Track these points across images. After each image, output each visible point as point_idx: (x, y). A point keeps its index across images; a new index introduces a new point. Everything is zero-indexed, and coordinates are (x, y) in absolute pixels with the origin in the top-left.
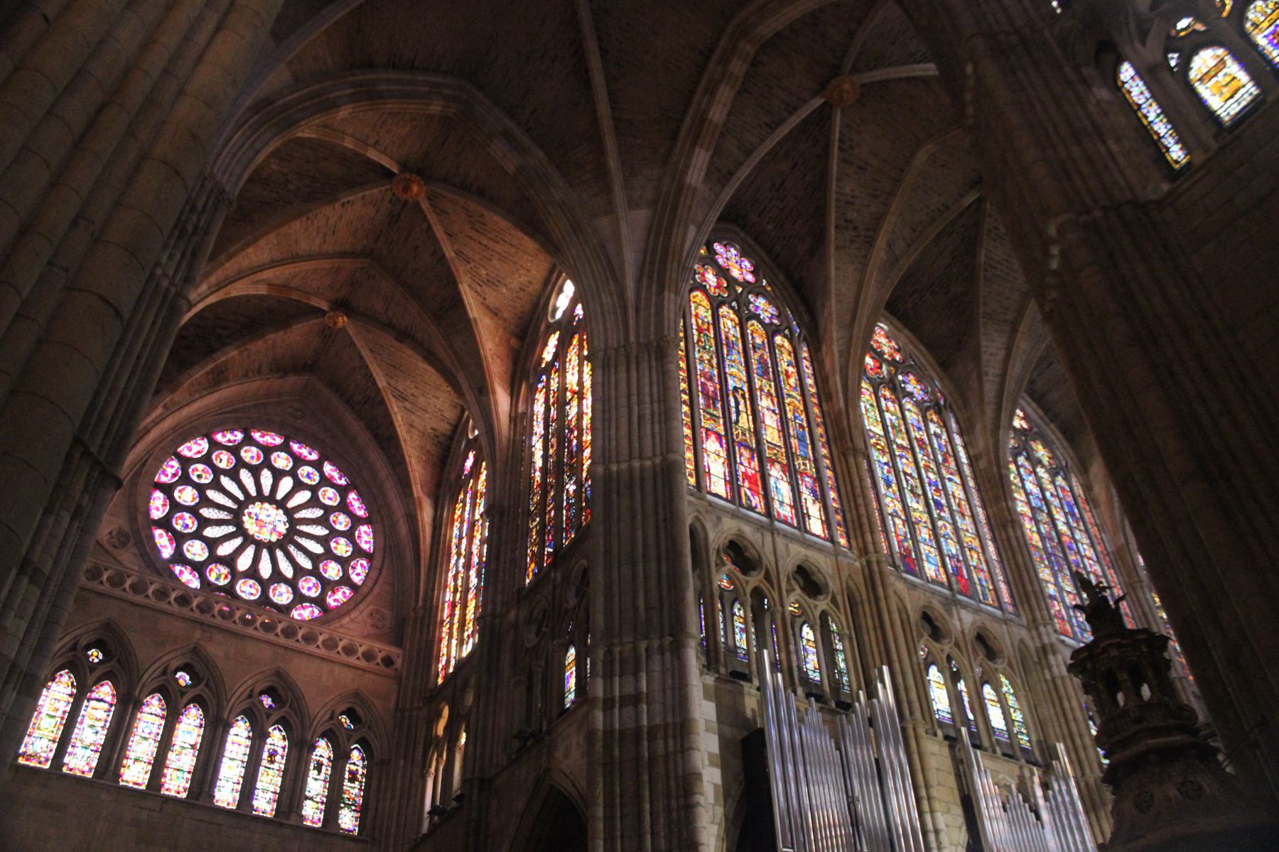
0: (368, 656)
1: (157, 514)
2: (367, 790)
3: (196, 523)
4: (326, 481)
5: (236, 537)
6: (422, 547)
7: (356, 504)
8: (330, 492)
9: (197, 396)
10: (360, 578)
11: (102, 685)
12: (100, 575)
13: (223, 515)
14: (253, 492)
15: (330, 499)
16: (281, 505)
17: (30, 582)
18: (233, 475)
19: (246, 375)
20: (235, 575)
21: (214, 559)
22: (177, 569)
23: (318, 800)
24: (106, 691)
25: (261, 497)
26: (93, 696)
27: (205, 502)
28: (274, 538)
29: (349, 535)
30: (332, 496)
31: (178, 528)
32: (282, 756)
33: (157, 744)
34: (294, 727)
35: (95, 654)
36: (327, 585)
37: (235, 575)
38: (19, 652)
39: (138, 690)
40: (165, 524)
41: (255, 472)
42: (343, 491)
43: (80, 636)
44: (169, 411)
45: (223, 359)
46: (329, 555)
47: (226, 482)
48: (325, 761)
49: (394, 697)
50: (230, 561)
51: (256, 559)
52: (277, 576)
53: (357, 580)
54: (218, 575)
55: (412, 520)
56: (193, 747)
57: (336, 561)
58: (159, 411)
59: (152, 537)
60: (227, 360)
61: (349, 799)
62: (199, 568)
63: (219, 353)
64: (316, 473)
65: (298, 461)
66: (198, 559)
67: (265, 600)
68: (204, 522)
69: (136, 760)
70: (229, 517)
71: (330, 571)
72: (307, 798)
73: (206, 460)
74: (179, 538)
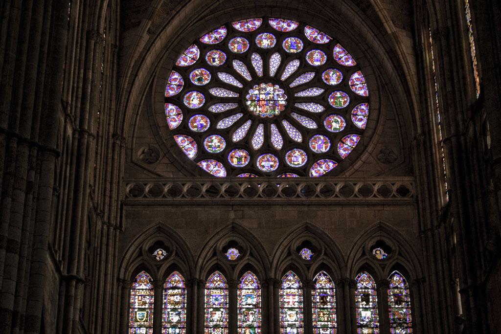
0: (384, 191)
1: (174, 125)
4: (310, 45)
5: (245, 122)
6: (408, 78)
9: (174, 12)
10: (363, 122)
12: (143, 190)
16: (275, 80)
17: (7, 252)
18: (228, 68)
20: (253, 155)
21: (232, 146)
22: (204, 164)
24: (177, 278)
25: (257, 80)
26: (169, 285)
27: (211, 100)
34: (333, 270)
35: (160, 252)
36: (335, 138)
38: (15, 302)
39: (198, 273)
40: (183, 130)
41: (245, 59)
42: (327, 49)
43: (142, 243)
44: (154, 34)
46: (330, 111)
49: (415, 222)
50: (245, 144)
51: (267, 135)
52: (289, 144)
53: (360, 124)
54: (238, 158)
55: (392, 54)
56: (256, 306)
57: (337, 114)
58: (146, 37)
59: (175, 144)
61: (399, 319)
62: (221, 158)
64: (299, 41)
65: (281, 36)
66: (218, 150)
67: (284, 168)
68: (215, 118)
71: (334, 124)
72: (362, 326)
74: (198, 138)
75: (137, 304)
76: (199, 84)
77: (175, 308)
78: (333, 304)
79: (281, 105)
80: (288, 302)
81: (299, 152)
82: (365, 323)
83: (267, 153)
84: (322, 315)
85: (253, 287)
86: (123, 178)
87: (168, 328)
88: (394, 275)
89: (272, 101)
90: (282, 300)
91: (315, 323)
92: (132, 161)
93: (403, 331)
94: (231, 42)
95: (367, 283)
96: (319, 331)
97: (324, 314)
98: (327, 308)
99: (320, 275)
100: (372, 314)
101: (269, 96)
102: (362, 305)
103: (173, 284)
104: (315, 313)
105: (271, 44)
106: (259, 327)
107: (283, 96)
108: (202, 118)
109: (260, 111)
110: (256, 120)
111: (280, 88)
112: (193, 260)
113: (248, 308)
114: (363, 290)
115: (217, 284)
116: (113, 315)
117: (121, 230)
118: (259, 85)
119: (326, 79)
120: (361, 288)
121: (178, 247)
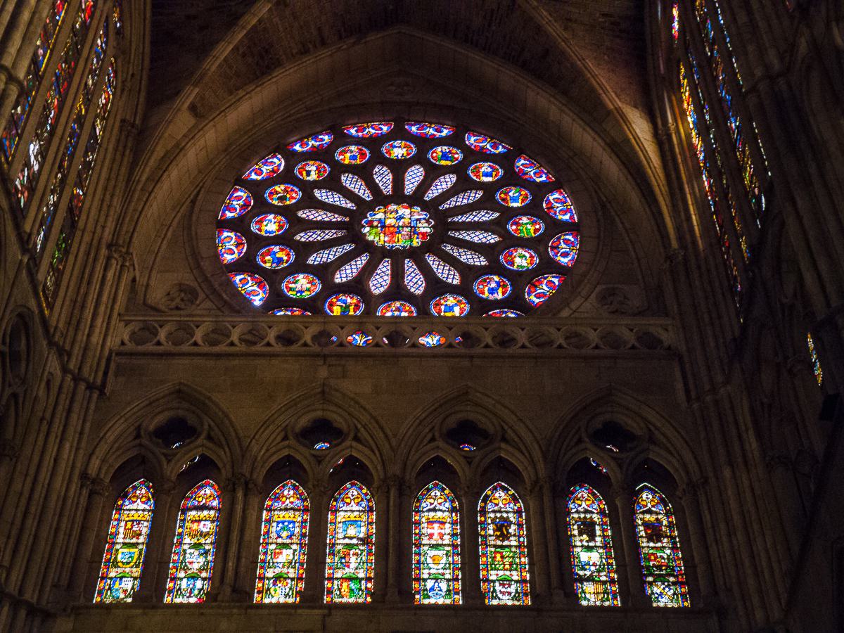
1: (228, 258)
2: (685, 546)
3: (292, 253)
5: (359, 255)
7: (531, 172)
8: (485, 167)
9: (241, 93)
11: (200, 488)
13: (329, 235)
14: (366, 195)
15: (486, 175)
18: (332, 183)
19: (305, 51)
23: (604, 579)
24: (207, 493)
25: (381, 200)
26: (190, 504)
28: (416, 242)
29: (533, 209)
30: (489, 170)
31: (268, 265)
32: (520, 525)
33: (305, 550)
37: (370, 301)
40: (247, 265)
41: (364, 172)
45: (254, 22)
47: (322, 195)
48: (596, 518)
51: (398, 274)
56: (365, 541)
59: (232, 285)
60: (260, 21)
61: (659, 567)
63: (247, 17)
65: (425, 144)
66: (306, 295)
69: (278, 578)
70: (339, 234)
71: (518, 261)
72: (582, 580)
73: (287, 177)
74: (272, 279)
75: (121, 536)
76: (280, 204)
77: (200, 544)
78: (522, 539)
79: (423, 234)
80: (431, 536)
81: (455, 299)
82: (588, 573)
83: (394, 300)
84: (498, 556)
85: (361, 509)
86: (119, 314)
87: (181, 579)
88: (642, 490)
89: (407, 227)
90: (417, 531)
91: (485, 573)
92: (145, 303)
93: (667, 589)
94: (340, 150)
95: (588, 503)
96: (494, 587)
97: (502, 557)
98: (510, 546)
99: (495, 489)
100: (601, 558)
101: (402, 220)
102: (581, 541)
103: (199, 502)
104: (485, 555)
105: (408, 154)
106: (368, 579)
107: (427, 221)
108: (282, 250)
109: (385, 242)
110: (378, 254)
111: (421, 211)
112: (240, 445)
113: (348, 544)
114: (582, 516)
115: (288, 502)
116: (61, 536)
117: (102, 393)
118: (386, 206)
119: (504, 200)
120: (578, 512)
121: (212, 424)
